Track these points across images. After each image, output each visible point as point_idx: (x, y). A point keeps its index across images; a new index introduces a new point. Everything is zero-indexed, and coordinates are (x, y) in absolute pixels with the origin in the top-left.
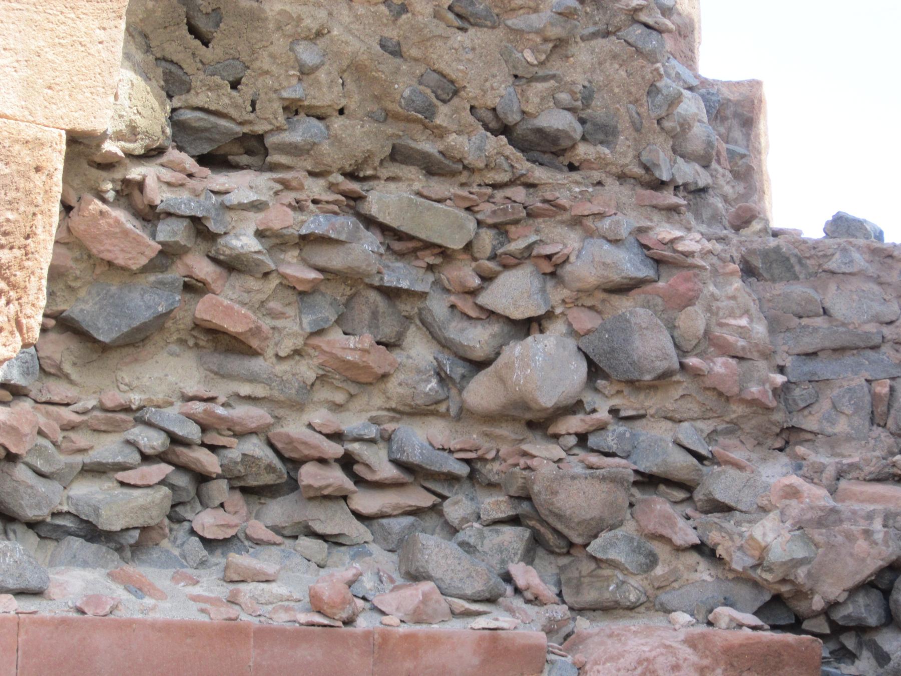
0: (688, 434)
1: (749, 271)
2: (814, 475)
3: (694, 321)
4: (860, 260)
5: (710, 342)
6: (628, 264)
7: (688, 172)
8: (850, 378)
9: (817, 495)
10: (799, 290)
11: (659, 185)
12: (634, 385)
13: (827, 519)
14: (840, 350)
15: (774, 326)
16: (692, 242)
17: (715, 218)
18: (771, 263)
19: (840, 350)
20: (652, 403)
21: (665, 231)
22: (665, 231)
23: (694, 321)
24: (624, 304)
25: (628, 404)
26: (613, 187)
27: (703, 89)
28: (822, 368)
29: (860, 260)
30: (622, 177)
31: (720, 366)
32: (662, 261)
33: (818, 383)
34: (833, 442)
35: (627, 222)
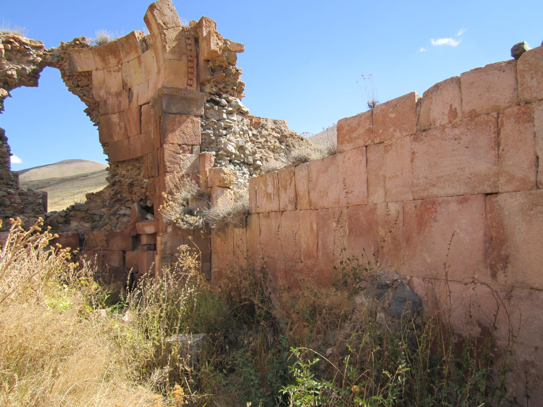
0: (11, 212)
1: (19, 195)
2: (26, 217)
3: (13, 200)
4: (32, 194)
5: (14, 202)
6: (5, 194)
7: (12, 183)
8: (30, 206)
9: (27, 219)
10: (25, 197)
11: (8, 185)
12: (5, 207)
13: (28, 221)
14: (29, 204)
15: (22, 201)
16: (13, 192)
17: (14, 188)
18: (21, 194)
19: (29, 204)
20: (7, 209)
21: (10, 190)
22: (10, 190)
23: (13, 200)
24: (5, 198)
25: (4, 209)
26: (3, 185)
27: (12, 172)
28: (27, 205)
29: (32, 194)
30: (4, 184)
31: (16, 205)
32: (9, 193)
33: (27, 207)
34: (28, 213)
35: (4, 189)
